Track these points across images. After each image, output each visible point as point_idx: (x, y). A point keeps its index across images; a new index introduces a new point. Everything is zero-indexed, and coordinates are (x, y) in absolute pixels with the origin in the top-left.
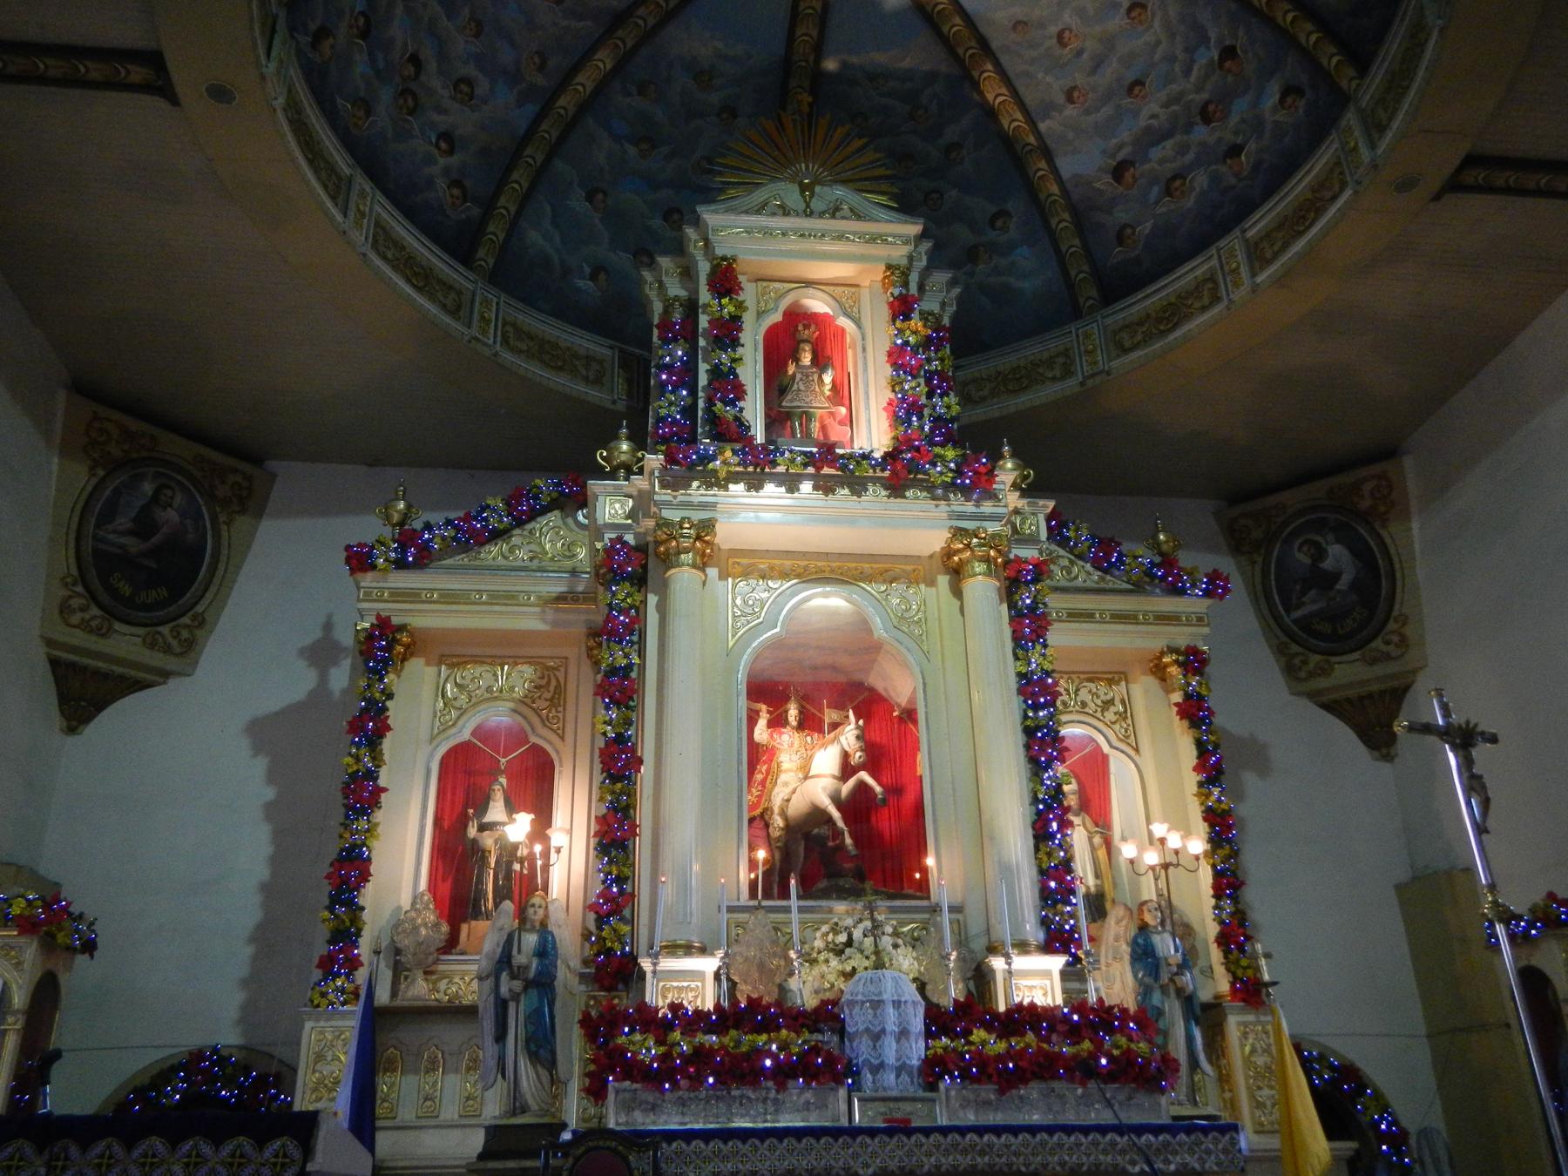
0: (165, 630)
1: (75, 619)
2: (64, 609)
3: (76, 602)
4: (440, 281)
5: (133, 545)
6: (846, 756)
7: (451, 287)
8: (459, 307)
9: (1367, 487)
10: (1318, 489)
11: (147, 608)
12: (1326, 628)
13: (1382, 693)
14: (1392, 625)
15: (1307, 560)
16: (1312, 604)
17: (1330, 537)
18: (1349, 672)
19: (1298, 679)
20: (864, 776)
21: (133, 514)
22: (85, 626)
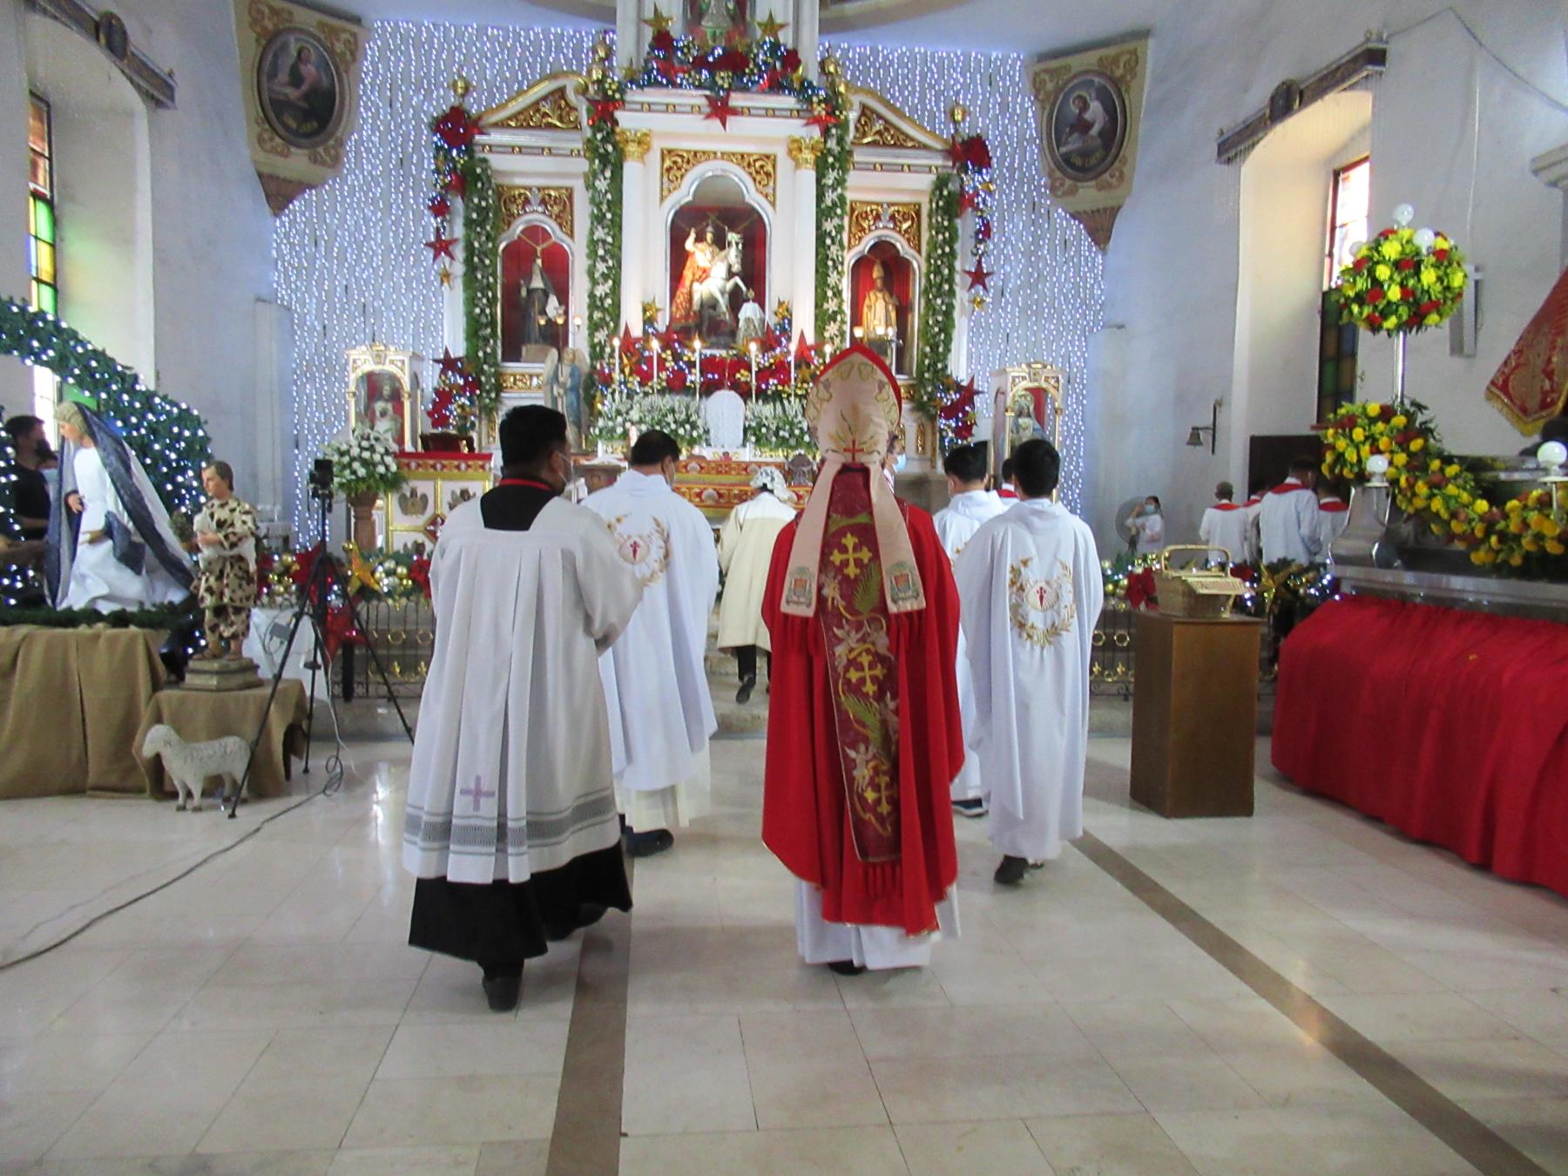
0: (321, 150)
1: (268, 146)
2: (261, 141)
3: (266, 136)
6: (730, 266)
9: (1124, 59)
10: (1091, 58)
11: (307, 136)
12: (1078, 161)
13: (1105, 210)
14: (1117, 164)
16: (1074, 143)
18: (1089, 195)
20: (737, 280)
21: (287, 71)
22: (273, 151)
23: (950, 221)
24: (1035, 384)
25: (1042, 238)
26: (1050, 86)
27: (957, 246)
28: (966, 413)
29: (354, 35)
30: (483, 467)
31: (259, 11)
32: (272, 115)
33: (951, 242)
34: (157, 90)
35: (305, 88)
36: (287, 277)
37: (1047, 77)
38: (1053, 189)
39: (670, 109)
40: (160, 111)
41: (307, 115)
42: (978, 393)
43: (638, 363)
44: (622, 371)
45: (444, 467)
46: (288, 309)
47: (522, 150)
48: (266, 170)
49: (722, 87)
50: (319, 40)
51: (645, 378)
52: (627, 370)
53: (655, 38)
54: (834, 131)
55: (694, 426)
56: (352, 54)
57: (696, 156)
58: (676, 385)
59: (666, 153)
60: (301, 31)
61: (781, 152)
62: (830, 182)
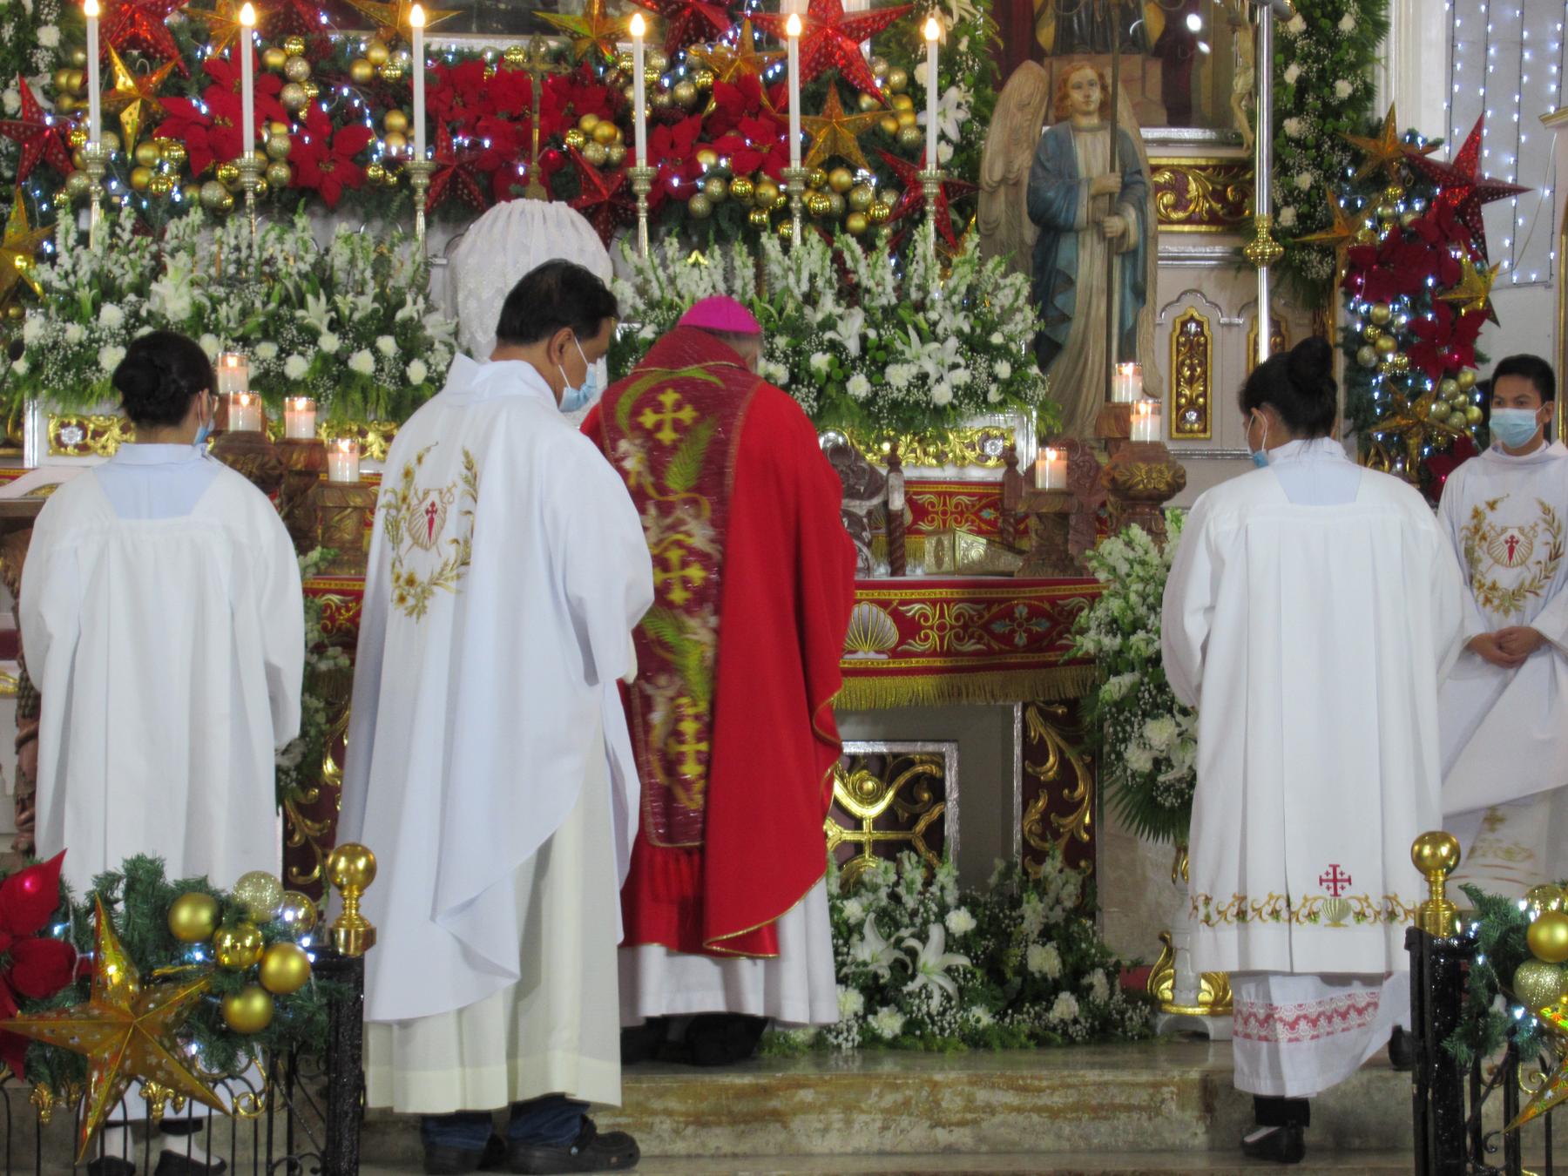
28: (1451, 275)
42: (1499, 191)
43: (174, 89)
44: (111, 122)
51: (208, 149)
52: (130, 117)
55: (413, 344)
58: (328, 175)
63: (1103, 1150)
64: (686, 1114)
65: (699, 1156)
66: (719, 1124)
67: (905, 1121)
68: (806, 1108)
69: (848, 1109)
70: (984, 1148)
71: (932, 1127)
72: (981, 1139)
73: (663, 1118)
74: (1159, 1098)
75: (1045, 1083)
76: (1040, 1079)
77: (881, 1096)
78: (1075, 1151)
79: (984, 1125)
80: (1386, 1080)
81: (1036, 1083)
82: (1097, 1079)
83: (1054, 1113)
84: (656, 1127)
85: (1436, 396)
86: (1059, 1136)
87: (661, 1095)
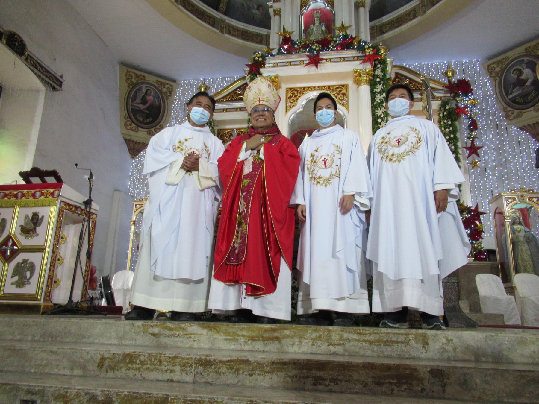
1: (129, 127)
2: (126, 125)
4: (207, 16)
5: (142, 107)
7: (211, 17)
8: (214, 23)
11: (147, 124)
12: (521, 100)
15: (515, 76)
16: (517, 92)
17: (525, 66)
19: (510, 120)
21: (141, 98)
22: (131, 129)
23: (452, 121)
24: (523, 206)
25: (503, 141)
26: (498, 69)
27: (458, 135)
28: (476, 225)
29: (172, 86)
30: (52, 194)
31: (130, 75)
32: (132, 115)
33: (454, 132)
34: (53, 82)
35: (148, 105)
36: (134, 183)
37: (495, 66)
38: (507, 116)
39: (290, 64)
40: (55, 93)
41: (147, 116)
45: (24, 195)
46: (133, 196)
47: (227, 110)
48: (128, 138)
49: (315, 50)
50: (156, 87)
53: (283, 40)
54: (379, 66)
56: (170, 92)
57: (305, 90)
59: (288, 90)
60: (148, 83)
61: (350, 82)
62: (378, 91)
63: (389, 357)
64: (249, 337)
65: (252, 351)
66: (259, 340)
67: (319, 343)
68: (287, 337)
69: (301, 337)
70: (347, 354)
71: (328, 345)
72: (346, 350)
73: (242, 337)
74: (408, 339)
75: (367, 332)
76: (366, 331)
77: (311, 334)
78: (379, 357)
79: (346, 345)
80: (492, 336)
81: (364, 332)
82: (386, 332)
83: (371, 343)
84: (239, 340)
85: (476, 244)
86: (373, 351)
87: (241, 330)
